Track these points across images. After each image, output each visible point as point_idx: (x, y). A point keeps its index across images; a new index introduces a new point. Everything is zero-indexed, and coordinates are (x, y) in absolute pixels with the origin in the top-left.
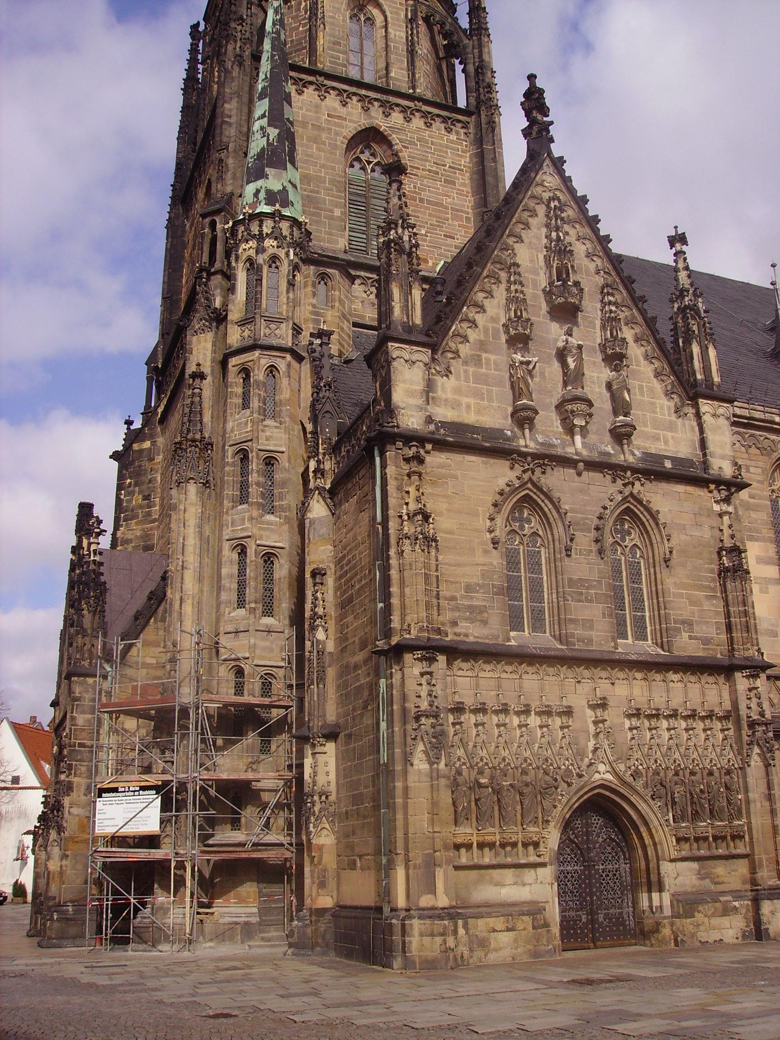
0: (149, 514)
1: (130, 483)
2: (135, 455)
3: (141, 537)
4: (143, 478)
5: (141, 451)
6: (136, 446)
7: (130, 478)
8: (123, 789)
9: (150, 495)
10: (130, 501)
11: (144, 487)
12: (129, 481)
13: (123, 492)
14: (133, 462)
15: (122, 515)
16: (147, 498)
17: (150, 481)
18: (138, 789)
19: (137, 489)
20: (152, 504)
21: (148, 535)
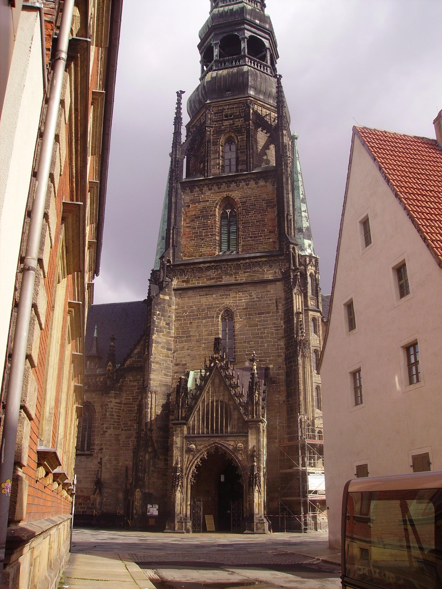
0: (169, 333)
1: (159, 314)
2: (161, 300)
3: (165, 343)
4: (166, 314)
5: (164, 300)
6: (161, 296)
7: (159, 312)
8: (316, 473)
9: (169, 324)
10: (159, 323)
11: (167, 318)
12: (158, 312)
13: (155, 317)
14: (160, 304)
15: (155, 328)
16: (168, 324)
17: (169, 317)
18: (321, 473)
19: (163, 318)
20: (171, 328)
21: (169, 343)
